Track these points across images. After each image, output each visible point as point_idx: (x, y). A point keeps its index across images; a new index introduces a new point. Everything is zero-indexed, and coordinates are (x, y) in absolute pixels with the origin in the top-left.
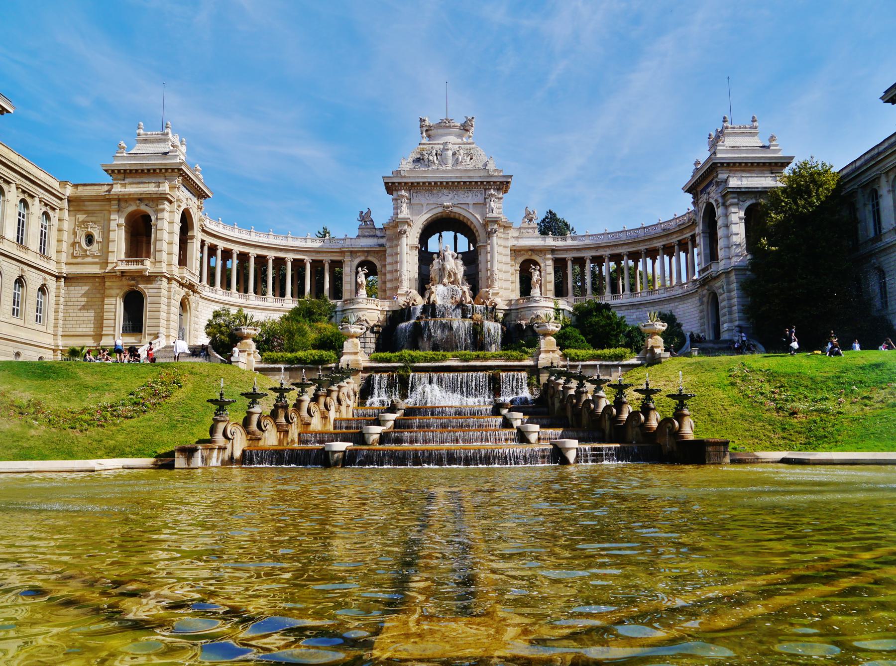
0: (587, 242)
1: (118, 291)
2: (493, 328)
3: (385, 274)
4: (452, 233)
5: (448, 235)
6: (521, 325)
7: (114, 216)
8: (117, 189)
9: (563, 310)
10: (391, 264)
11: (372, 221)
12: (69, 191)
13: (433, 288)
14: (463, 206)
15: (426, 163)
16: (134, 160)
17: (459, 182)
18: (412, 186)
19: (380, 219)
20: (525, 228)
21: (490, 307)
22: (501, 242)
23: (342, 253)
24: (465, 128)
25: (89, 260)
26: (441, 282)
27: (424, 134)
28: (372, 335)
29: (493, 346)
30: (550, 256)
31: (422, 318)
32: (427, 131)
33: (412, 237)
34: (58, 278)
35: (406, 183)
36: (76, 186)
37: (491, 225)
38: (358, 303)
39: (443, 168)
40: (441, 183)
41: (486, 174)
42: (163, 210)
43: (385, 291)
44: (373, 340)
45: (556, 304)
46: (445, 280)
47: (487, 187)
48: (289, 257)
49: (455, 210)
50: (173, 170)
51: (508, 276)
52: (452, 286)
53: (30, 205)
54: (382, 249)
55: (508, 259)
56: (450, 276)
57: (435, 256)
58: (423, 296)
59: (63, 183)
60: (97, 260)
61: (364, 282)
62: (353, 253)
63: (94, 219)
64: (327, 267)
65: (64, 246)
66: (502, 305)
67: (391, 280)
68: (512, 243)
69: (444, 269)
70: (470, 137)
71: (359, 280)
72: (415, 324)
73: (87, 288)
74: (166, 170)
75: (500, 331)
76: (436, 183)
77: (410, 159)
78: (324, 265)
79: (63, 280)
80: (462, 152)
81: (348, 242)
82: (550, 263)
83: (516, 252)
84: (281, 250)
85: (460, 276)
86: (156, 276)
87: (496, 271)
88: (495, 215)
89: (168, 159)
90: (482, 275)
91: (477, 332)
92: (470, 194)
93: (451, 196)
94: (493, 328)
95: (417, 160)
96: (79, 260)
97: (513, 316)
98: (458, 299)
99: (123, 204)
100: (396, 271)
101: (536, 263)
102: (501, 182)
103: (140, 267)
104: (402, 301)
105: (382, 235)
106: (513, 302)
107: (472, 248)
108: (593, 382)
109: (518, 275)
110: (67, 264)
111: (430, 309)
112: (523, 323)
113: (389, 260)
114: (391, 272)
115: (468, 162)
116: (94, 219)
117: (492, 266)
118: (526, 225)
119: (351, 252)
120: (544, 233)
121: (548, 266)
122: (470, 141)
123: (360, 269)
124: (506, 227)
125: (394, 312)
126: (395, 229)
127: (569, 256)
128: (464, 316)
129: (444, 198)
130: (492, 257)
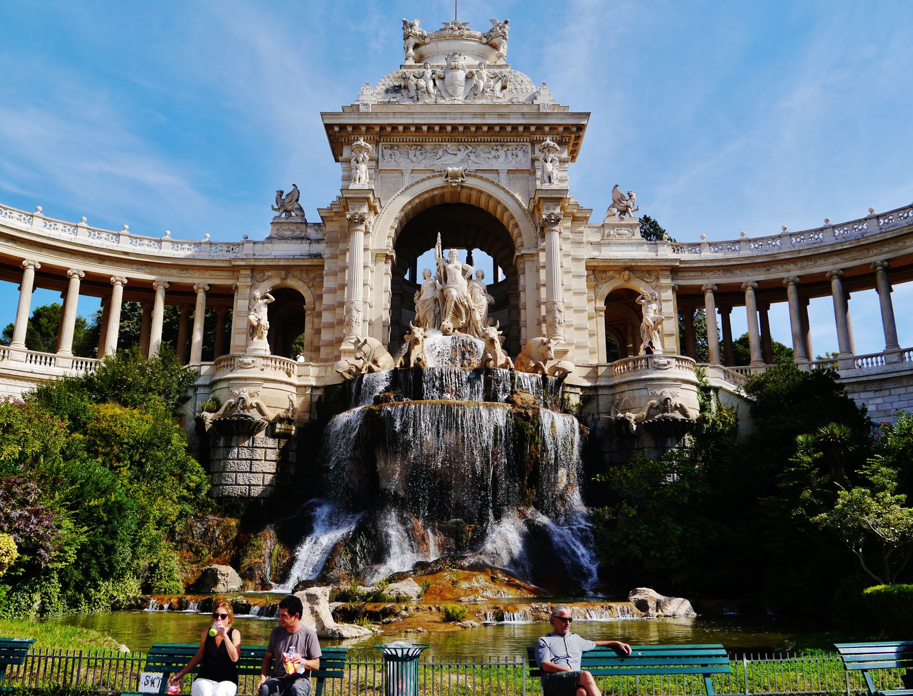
0: (745, 252)
2: (560, 427)
3: (319, 315)
6: (625, 422)
9: (716, 390)
10: (332, 291)
11: (301, 209)
13: (418, 332)
14: (486, 176)
15: (413, 93)
17: (478, 127)
18: (383, 134)
19: (316, 201)
20: (613, 226)
21: (552, 379)
22: (567, 247)
23: (234, 270)
24: (490, 42)
26: (437, 323)
28: (271, 443)
29: (562, 472)
30: (666, 281)
31: (386, 400)
32: (416, 46)
33: (378, 234)
35: (369, 127)
37: (548, 211)
38: (244, 366)
39: (448, 101)
40: (442, 127)
41: (534, 110)
43: (317, 350)
44: (272, 455)
45: (700, 375)
46: (448, 323)
47: (537, 137)
48: (120, 275)
49: (470, 182)
51: (582, 320)
52: (463, 336)
54: (315, 262)
55: (582, 284)
56: (457, 313)
58: (393, 348)
61: (265, 322)
62: (256, 271)
64: (201, 298)
66: (577, 377)
67: (331, 326)
68: (588, 253)
69: (444, 299)
70: (500, 56)
72: (369, 417)
75: (577, 437)
76: (430, 127)
77: (381, 88)
78: (195, 295)
80: (485, 72)
81: (248, 249)
82: (669, 295)
83: (597, 271)
84: (101, 259)
85: (480, 314)
87: (561, 306)
88: (556, 185)
90: (527, 316)
91: (523, 432)
92: (502, 153)
93: (462, 155)
94: (560, 427)
95: (397, 89)
97: (603, 402)
98: (476, 362)
100: (341, 304)
102: (567, 128)
104: (345, 364)
105: (319, 236)
106: (601, 371)
107: (501, 277)
109: (602, 320)
111: (409, 380)
112: (632, 416)
113: (328, 283)
114: (331, 308)
115: (498, 94)
117: (551, 292)
118: (615, 220)
119: (253, 268)
122: (501, 62)
124: (579, 218)
125: (328, 389)
126: (345, 216)
128: (490, 397)
129: (447, 159)
130: (550, 275)
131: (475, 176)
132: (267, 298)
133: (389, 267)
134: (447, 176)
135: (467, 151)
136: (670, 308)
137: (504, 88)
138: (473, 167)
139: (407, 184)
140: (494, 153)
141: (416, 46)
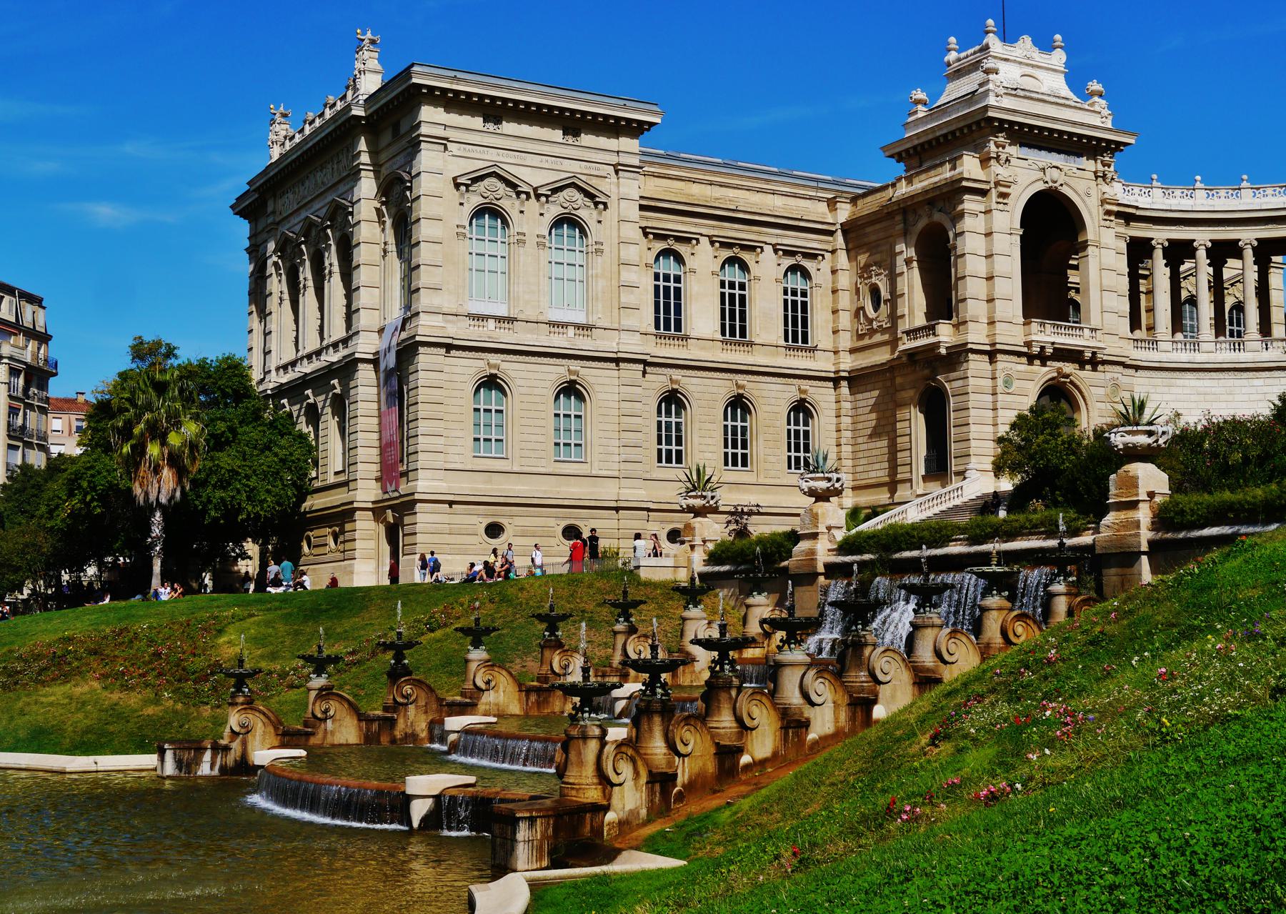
1: (911, 393)
7: (900, 247)
8: (903, 189)
12: (844, 213)
16: (964, 108)
25: (878, 338)
34: (836, 381)
36: (854, 200)
42: (961, 215)
50: (978, 123)
53: (751, 264)
59: (832, 204)
60: (886, 337)
63: (877, 257)
65: (845, 320)
73: (876, 393)
74: (969, 126)
79: (844, 383)
86: (959, 353)
89: (977, 103)
96: (866, 341)
99: (911, 218)
103: (931, 340)
110: (852, 351)
116: (877, 257)
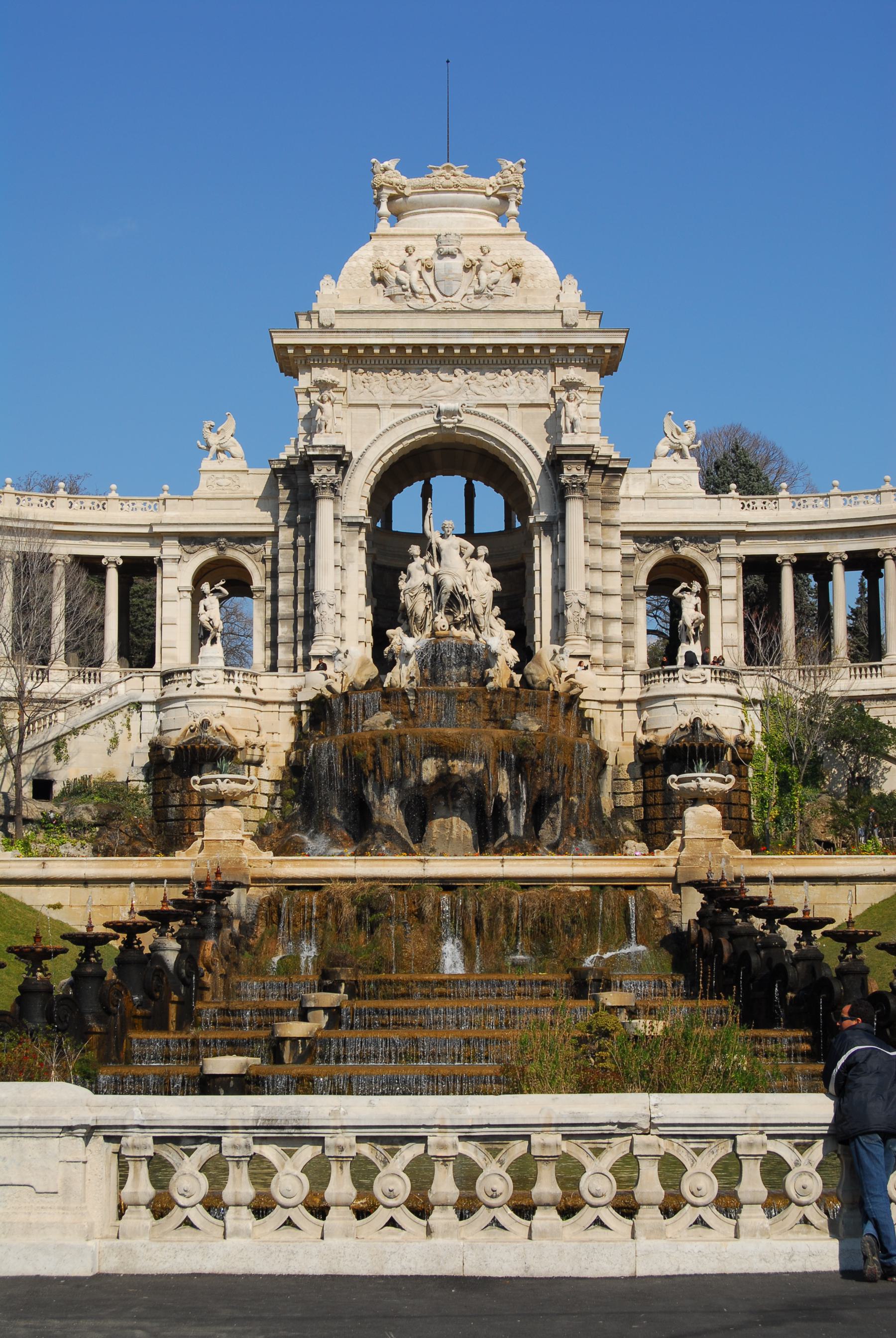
4: (458, 482)
5: (449, 487)
23: (155, 538)
27: (384, 209)
32: (391, 198)
41: (556, 324)
57: (415, 550)
61: (218, 623)
71: (204, 618)
82: (733, 568)
88: (579, 440)
101: (694, 572)
108: (794, 924)
120: (714, 485)
121: (727, 584)
123: (206, 587)
127: (783, 550)
131: (475, 414)
132: (219, 591)
133: (362, 537)
134: (439, 413)
135: (466, 376)
136: (733, 587)
137: (516, 279)
138: (474, 400)
139: (386, 425)
140: (501, 378)
141: (391, 198)
